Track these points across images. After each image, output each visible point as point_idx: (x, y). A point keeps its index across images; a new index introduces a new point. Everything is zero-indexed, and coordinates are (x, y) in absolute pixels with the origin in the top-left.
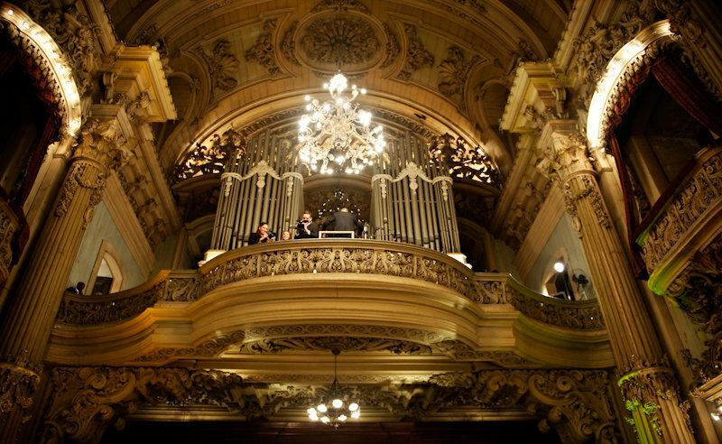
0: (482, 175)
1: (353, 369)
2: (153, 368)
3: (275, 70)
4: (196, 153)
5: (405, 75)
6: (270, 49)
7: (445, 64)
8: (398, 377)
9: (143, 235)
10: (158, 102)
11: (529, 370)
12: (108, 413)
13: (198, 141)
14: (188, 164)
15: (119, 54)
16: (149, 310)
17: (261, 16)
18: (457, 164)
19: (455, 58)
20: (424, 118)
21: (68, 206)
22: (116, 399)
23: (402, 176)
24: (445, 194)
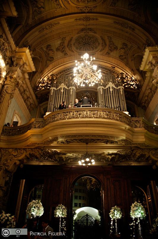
0: (134, 86)
1: (93, 149)
2: (31, 149)
3: (66, 54)
4: (42, 82)
5: (108, 54)
6: (64, 47)
7: (121, 49)
8: (107, 152)
9: (27, 108)
10: (30, 65)
11: (149, 148)
12: (18, 163)
13: (42, 78)
14: (40, 86)
15: (17, 51)
16: (29, 131)
17: (61, 36)
18: (125, 82)
19: (124, 47)
20: (114, 68)
21: (3, 99)
22: (20, 158)
23: (107, 87)
24: (122, 92)
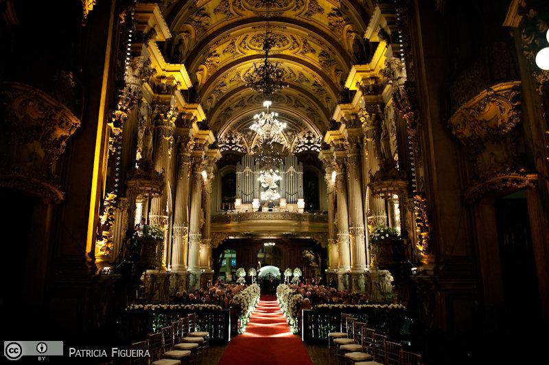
12: (221, 243)
18: (313, 144)
23: (288, 171)
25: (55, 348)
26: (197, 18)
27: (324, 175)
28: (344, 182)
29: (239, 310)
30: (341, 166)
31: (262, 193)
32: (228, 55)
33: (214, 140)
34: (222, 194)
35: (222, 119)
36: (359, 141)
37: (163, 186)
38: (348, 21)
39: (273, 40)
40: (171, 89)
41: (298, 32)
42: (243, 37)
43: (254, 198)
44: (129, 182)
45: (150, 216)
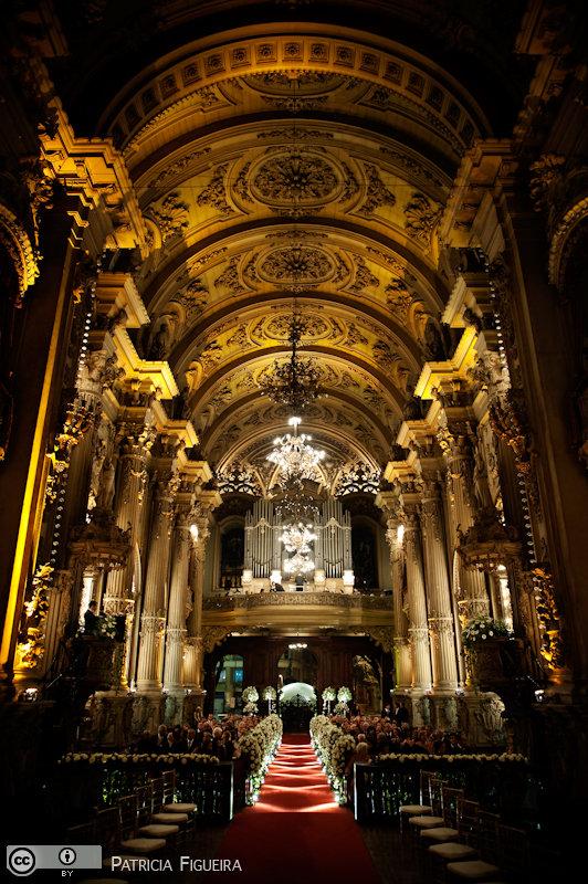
12: (219, 643)
22: (220, 638)
25: (88, 856)
26: (189, 294)
27: (386, 532)
28: (417, 542)
29: (248, 764)
30: (412, 517)
31: (286, 561)
32: (234, 347)
33: (210, 476)
34: (222, 562)
35: (223, 443)
36: (439, 478)
37: (127, 552)
38: (417, 296)
39: (303, 325)
40: (146, 399)
41: (342, 314)
42: (258, 320)
43: (273, 568)
44: (75, 545)
45: (106, 600)
